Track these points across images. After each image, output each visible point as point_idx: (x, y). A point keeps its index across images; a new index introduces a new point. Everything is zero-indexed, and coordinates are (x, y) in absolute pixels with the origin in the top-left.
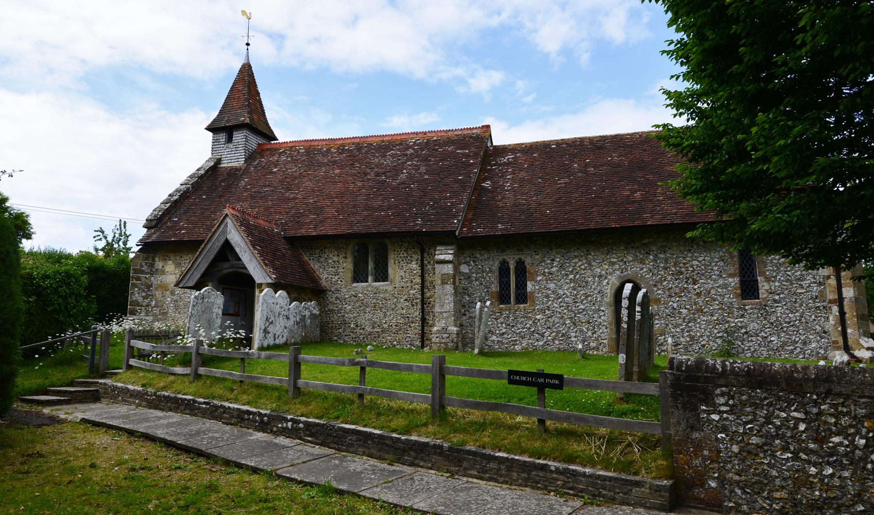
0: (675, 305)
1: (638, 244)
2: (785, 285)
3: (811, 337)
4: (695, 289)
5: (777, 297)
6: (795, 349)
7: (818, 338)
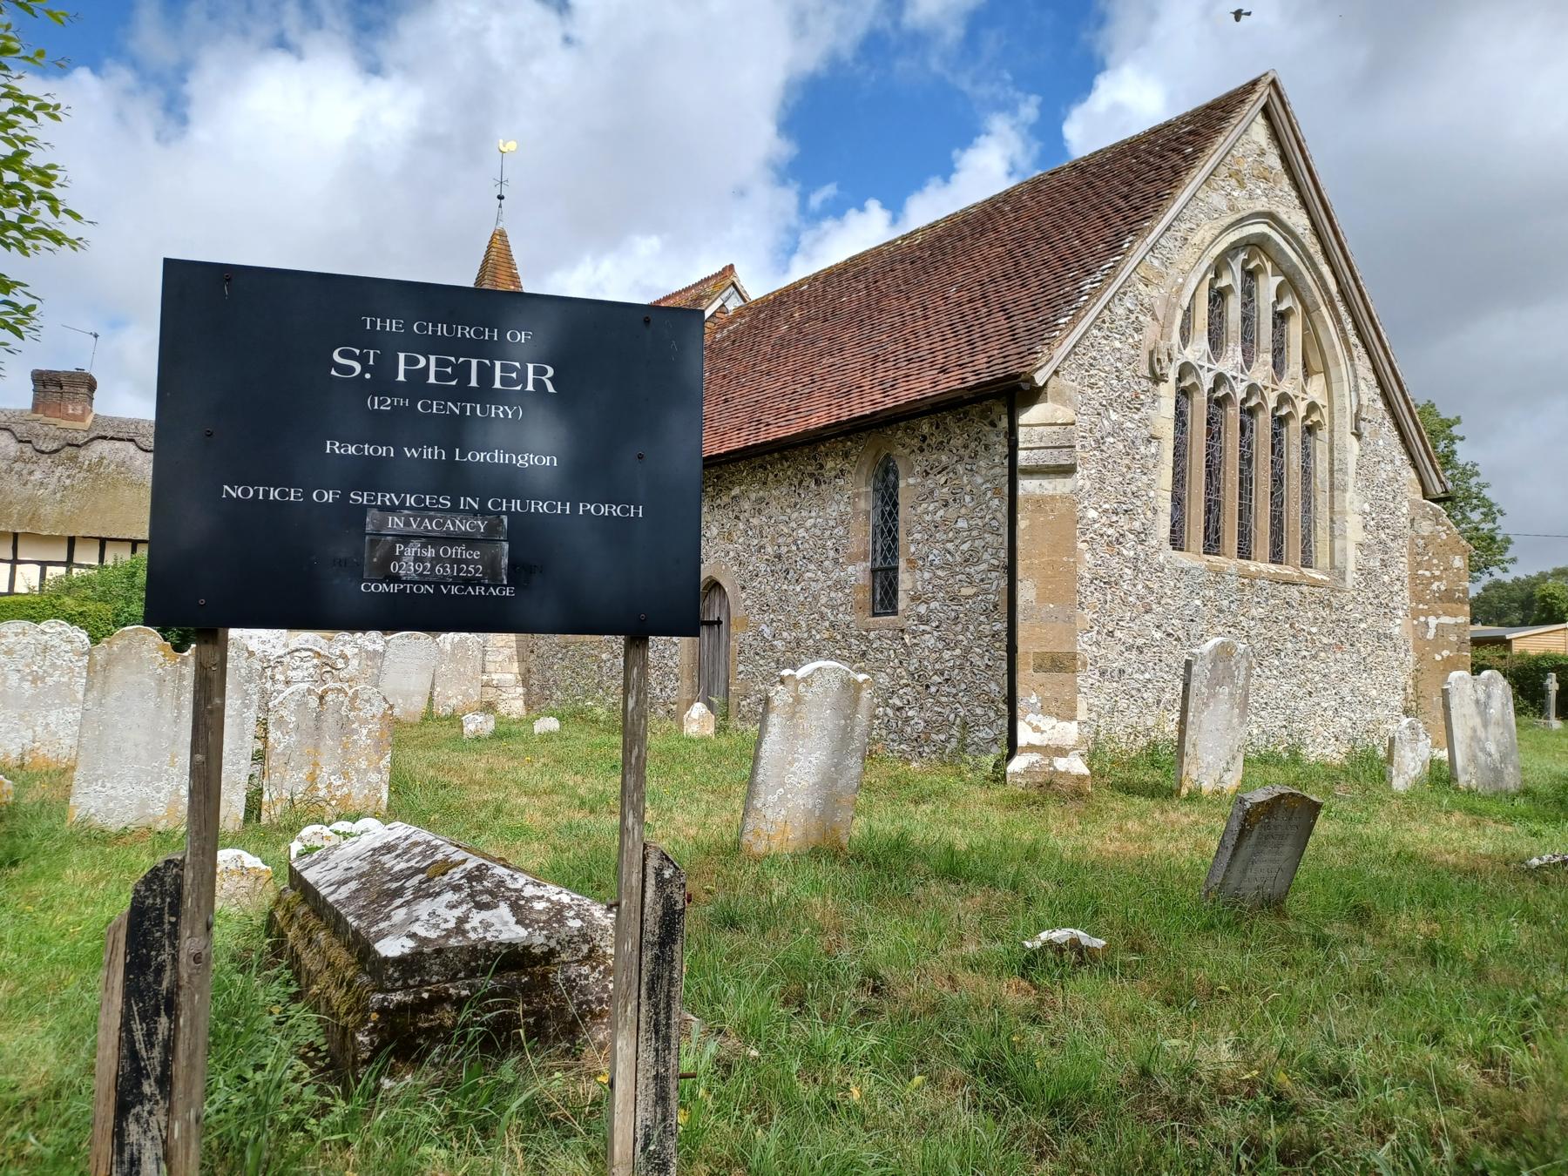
0: (767, 632)
1: (726, 499)
2: (940, 578)
3: (979, 711)
4: (797, 594)
5: (922, 609)
6: (948, 740)
7: (992, 714)
